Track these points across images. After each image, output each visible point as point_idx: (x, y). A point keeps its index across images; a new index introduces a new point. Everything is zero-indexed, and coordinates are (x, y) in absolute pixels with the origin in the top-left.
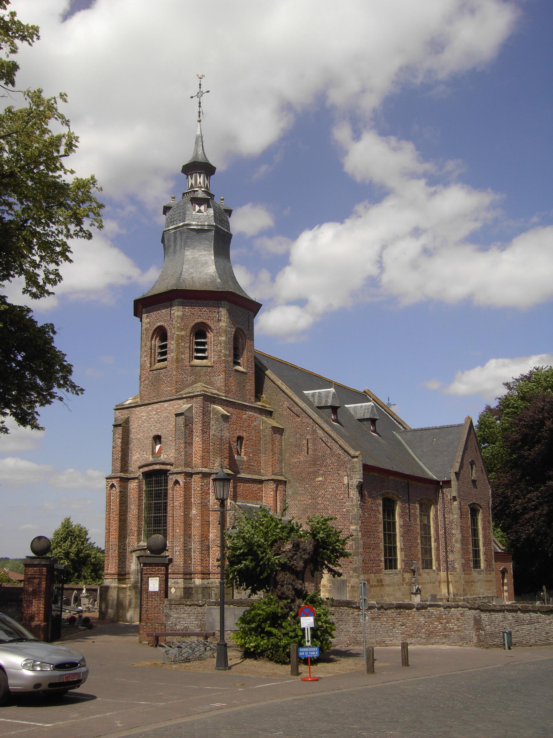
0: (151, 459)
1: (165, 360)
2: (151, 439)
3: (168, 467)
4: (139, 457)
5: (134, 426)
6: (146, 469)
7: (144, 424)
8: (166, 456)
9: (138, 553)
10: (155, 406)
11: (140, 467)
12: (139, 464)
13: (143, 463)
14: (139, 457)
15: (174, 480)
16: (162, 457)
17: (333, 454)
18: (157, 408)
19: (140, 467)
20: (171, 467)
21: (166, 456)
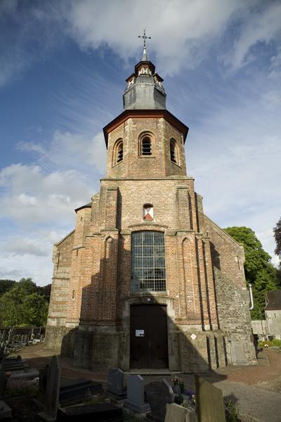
0: (142, 221)
1: (151, 154)
2: (142, 207)
3: (162, 229)
4: (130, 219)
5: (123, 194)
6: (136, 229)
7: (134, 194)
8: (158, 221)
9: (132, 301)
10: (146, 182)
11: (130, 227)
12: (128, 224)
13: (134, 224)
14: (130, 219)
15: (184, 237)
16: (155, 221)
17: (225, 243)
18: (147, 184)
19: (130, 227)
20: (166, 229)
21: (158, 221)
